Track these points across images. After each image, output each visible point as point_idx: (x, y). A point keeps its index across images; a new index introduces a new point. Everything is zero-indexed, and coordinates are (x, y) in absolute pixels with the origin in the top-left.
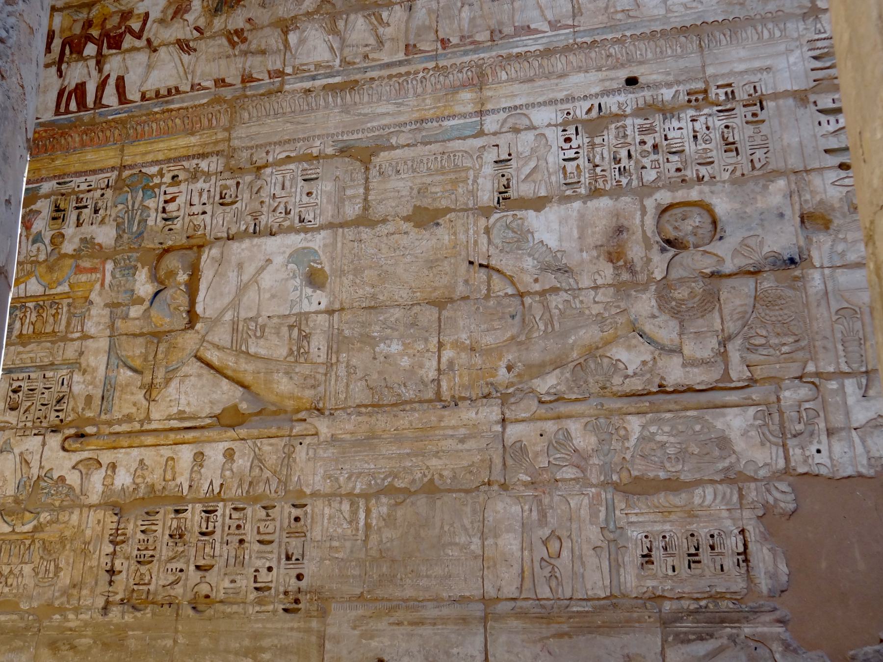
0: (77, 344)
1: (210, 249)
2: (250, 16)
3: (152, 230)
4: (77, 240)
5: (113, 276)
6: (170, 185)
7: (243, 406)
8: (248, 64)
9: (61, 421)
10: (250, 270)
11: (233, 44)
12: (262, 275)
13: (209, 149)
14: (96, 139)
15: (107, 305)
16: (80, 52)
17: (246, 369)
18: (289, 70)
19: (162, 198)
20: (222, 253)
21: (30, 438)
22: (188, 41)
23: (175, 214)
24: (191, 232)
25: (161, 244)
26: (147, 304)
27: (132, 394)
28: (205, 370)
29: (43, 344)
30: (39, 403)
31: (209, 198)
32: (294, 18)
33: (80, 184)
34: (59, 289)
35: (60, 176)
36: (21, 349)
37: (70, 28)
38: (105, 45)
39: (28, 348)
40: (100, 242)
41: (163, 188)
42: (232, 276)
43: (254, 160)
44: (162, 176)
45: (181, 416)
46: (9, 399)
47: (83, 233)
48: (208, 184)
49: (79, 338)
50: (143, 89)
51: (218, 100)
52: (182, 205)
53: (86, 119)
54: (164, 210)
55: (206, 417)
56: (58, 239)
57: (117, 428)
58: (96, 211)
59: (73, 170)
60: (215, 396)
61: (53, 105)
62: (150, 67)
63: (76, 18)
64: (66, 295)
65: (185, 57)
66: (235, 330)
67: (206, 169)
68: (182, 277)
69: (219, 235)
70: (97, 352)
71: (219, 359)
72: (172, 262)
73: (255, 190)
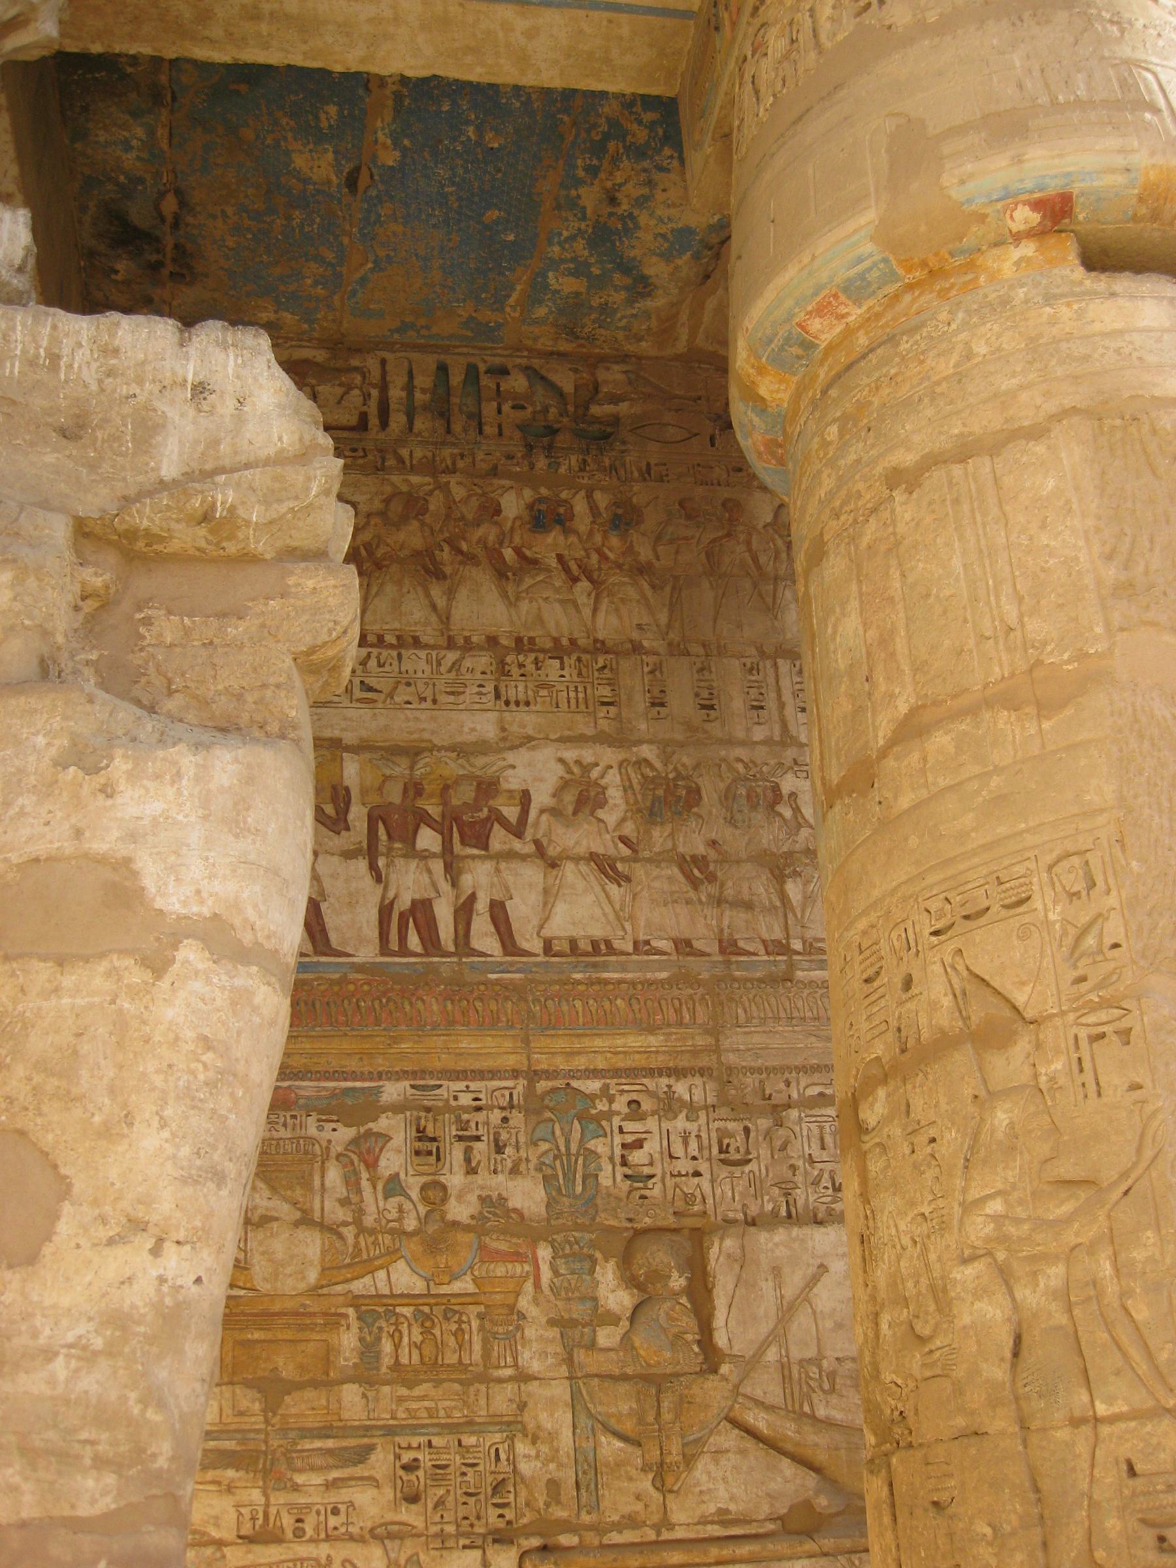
0: (510, 1388)
1: (722, 1239)
2: (713, 836)
3: (609, 1195)
4: (473, 1198)
5: (556, 1273)
6: (627, 1118)
7: (822, 1502)
8: (726, 922)
9: (509, 1523)
10: (794, 1281)
11: (695, 884)
12: (815, 1290)
13: (684, 1062)
14: (472, 1013)
15: (552, 1323)
16: (410, 839)
17: (817, 1443)
18: (797, 945)
19: (618, 1140)
20: (743, 1247)
21: (455, 1554)
22: (615, 860)
23: (647, 1170)
24: (680, 1205)
25: (630, 1220)
26: (625, 1324)
27: (630, 1479)
28: (750, 1444)
29: (446, 1385)
30: (459, 1492)
31: (701, 1149)
32: (790, 854)
33: (460, 1093)
34: (457, 1287)
35: (414, 1073)
36: (403, 1391)
37: (380, 789)
38: (456, 835)
39: (418, 1391)
40: (518, 1206)
41: (616, 1121)
42: (767, 1287)
43: (767, 1092)
44: (611, 1100)
45: (723, 1518)
46: (399, 1482)
47: (482, 1188)
48: (696, 1124)
49: (510, 1379)
50: (547, 932)
51: (683, 978)
52: (657, 1156)
53: (445, 972)
54: (624, 1163)
55: (765, 1520)
56: (434, 1192)
57: (615, 1538)
58: (499, 1149)
59: (438, 1065)
60: (773, 1486)
61: (373, 933)
62: (549, 896)
63: (388, 772)
64: (467, 1299)
65: (613, 889)
66: (786, 1378)
67: (687, 1097)
68: (678, 1282)
69: (731, 1215)
70: (552, 1403)
71: (769, 1425)
72: (658, 1255)
73: (778, 1143)
